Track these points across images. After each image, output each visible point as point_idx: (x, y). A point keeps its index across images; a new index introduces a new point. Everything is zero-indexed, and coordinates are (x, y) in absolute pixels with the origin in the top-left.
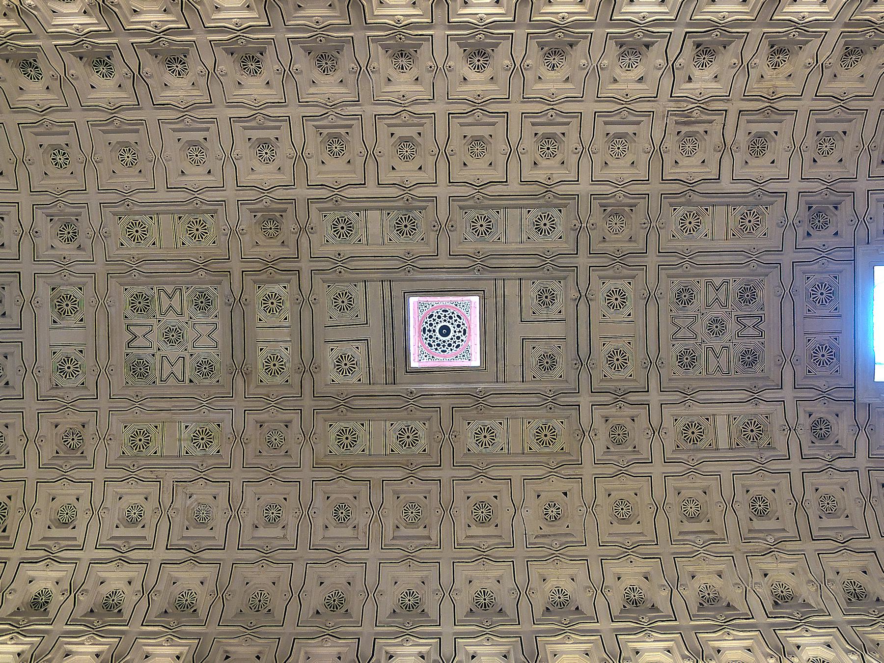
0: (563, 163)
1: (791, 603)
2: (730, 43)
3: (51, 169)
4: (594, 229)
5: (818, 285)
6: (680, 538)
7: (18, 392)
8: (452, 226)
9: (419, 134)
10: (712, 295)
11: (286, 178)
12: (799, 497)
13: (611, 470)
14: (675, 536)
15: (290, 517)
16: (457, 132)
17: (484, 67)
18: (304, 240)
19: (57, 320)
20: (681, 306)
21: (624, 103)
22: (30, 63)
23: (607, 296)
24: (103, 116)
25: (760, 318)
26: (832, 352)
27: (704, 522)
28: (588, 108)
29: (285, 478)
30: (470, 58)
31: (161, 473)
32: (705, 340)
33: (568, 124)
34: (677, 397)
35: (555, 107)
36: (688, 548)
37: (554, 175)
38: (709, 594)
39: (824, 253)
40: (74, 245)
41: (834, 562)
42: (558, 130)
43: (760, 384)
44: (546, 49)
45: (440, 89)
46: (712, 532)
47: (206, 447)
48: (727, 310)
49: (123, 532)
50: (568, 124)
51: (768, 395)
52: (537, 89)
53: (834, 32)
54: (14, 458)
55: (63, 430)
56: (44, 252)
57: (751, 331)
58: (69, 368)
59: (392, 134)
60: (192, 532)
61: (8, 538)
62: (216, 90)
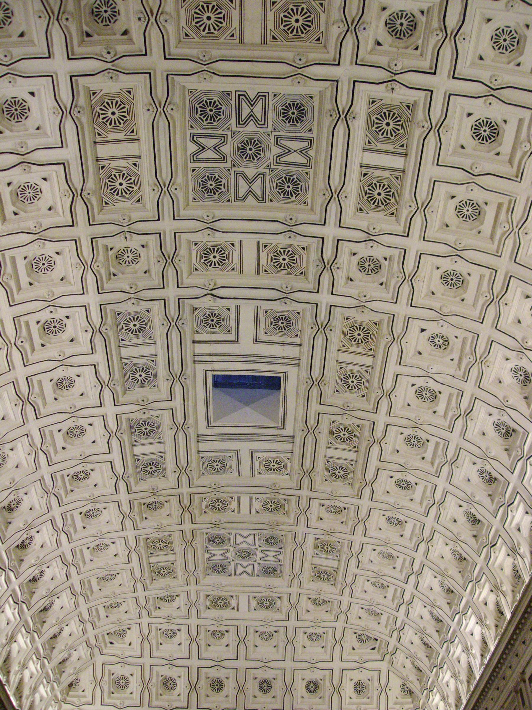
5: (197, 23)
10: (209, 154)
13: (406, 289)
20: (223, 190)
23: (210, 265)
25: (241, 97)
26: (292, 10)
29: (366, 515)
32: (266, 164)
34: (333, 207)
43: (328, 105)
48: (229, 137)
51: (343, 101)
57: (258, 110)
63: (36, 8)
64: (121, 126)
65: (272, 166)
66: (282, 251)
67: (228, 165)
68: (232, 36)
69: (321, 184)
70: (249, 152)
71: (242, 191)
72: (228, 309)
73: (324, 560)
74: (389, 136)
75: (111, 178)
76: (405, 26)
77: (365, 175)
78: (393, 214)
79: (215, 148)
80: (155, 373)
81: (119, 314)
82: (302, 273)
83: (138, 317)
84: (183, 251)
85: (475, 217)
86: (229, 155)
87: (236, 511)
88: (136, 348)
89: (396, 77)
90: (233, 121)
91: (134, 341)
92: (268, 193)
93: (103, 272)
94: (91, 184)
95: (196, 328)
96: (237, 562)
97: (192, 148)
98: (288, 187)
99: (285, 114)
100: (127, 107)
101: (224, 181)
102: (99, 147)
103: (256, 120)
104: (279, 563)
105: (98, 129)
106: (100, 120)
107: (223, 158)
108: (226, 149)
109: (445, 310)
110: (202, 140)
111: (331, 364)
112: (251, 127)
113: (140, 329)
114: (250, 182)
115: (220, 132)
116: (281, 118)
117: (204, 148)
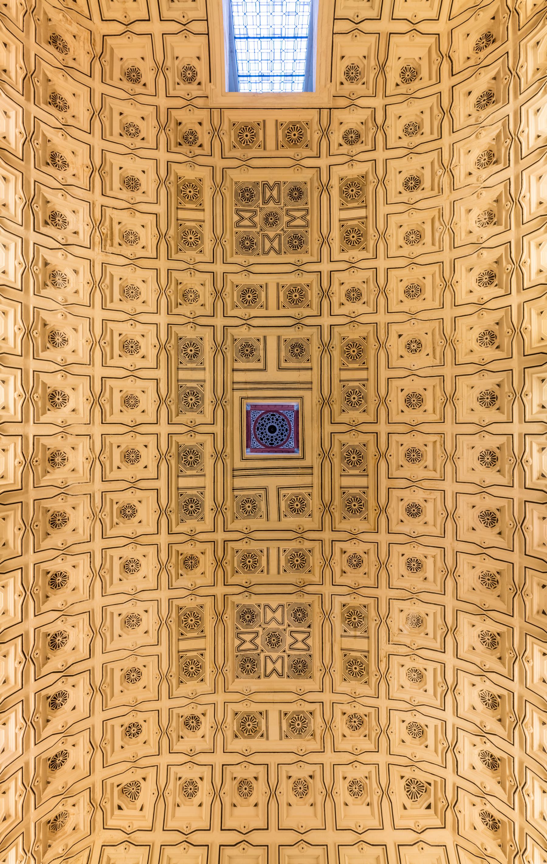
0: (143, 336)
1: (495, 151)
2: (44, 197)
3: (142, 737)
4: (195, 312)
5: (240, 139)
6: (437, 244)
7: (317, 768)
8: (191, 422)
9: (118, 446)
10: (246, 223)
11: (152, 551)
12: (405, 151)
13: (382, 300)
14: (436, 248)
15: (418, 552)
16: (117, 417)
17: (64, 395)
18: (201, 537)
19: (260, 734)
20: (255, 247)
21: (95, 286)
22: (52, 762)
23: (246, 303)
24: (98, 697)
26: (292, 128)
27: (425, 226)
28: (98, 314)
29: (386, 555)
30: (56, 406)
31: (382, 654)
33: (112, 331)
34: (325, 249)
35: (98, 340)
36: (447, 238)
37: (153, 343)
38: (485, 219)
39: (215, 132)
40: (202, 718)
41: (460, 120)
42: (117, 339)
43: (316, 184)
44: (48, 345)
45: (83, 430)
46: (433, 220)
47: (361, 616)
49: (430, 686)
50: (112, 331)
51: (324, 179)
52: (83, 355)
53: (34, 111)
54: (370, 772)
55: (348, 730)
56: (207, 745)
57: (275, 193)
58: (298, 725)
59: (119, 468)
60: (430, 630)
61: (435, 782)
62: (78, 608)
63: (153, 124)
64: (194, 200)
65: (285, 229)
66: (294, 289)
67: (258, 230)
68: (259, 146)
69: (316, 235)
70: (270, 220)
71: (267, 247)
72: (258, 340)
73: (352, 639)
74: (354, 197)
75: (185, 233)
76: (354, 138)
77: (343, 226)
78: (364, 248)
79: (250, 219)
80: (202, 399)
81: (180, 339)
82: (308, 306)
83: (194, 343)
84: (228, 289)
85: (418, 240)
86: (258, 223)
87: (265, 571)
88: (190, 372)
89: (353, 158)
90: (261, 201)
91: (189, 365)
92: (283, 248)
93: (173, 298)
94: (172, 232)
95: (236, 358)
96: (267, 654)
97: (236, 218)
98: (296, 242)
99: (291, 195)
100: (198, 189)
101: (255, 241)
102: (180, 212)
103: (274, 200)
104: (309, 653)
105: (180, 200)
106: (182, 195)
107: (255, 226)
108: (256, 219)
109: (414, 310)
110: (242, 213)
111: (336, 381)
112: (271, 204)
113: (195, 355)
114: (271, 241)
115: (253, 208)
116: (289, 197)
117: (243, 218)
